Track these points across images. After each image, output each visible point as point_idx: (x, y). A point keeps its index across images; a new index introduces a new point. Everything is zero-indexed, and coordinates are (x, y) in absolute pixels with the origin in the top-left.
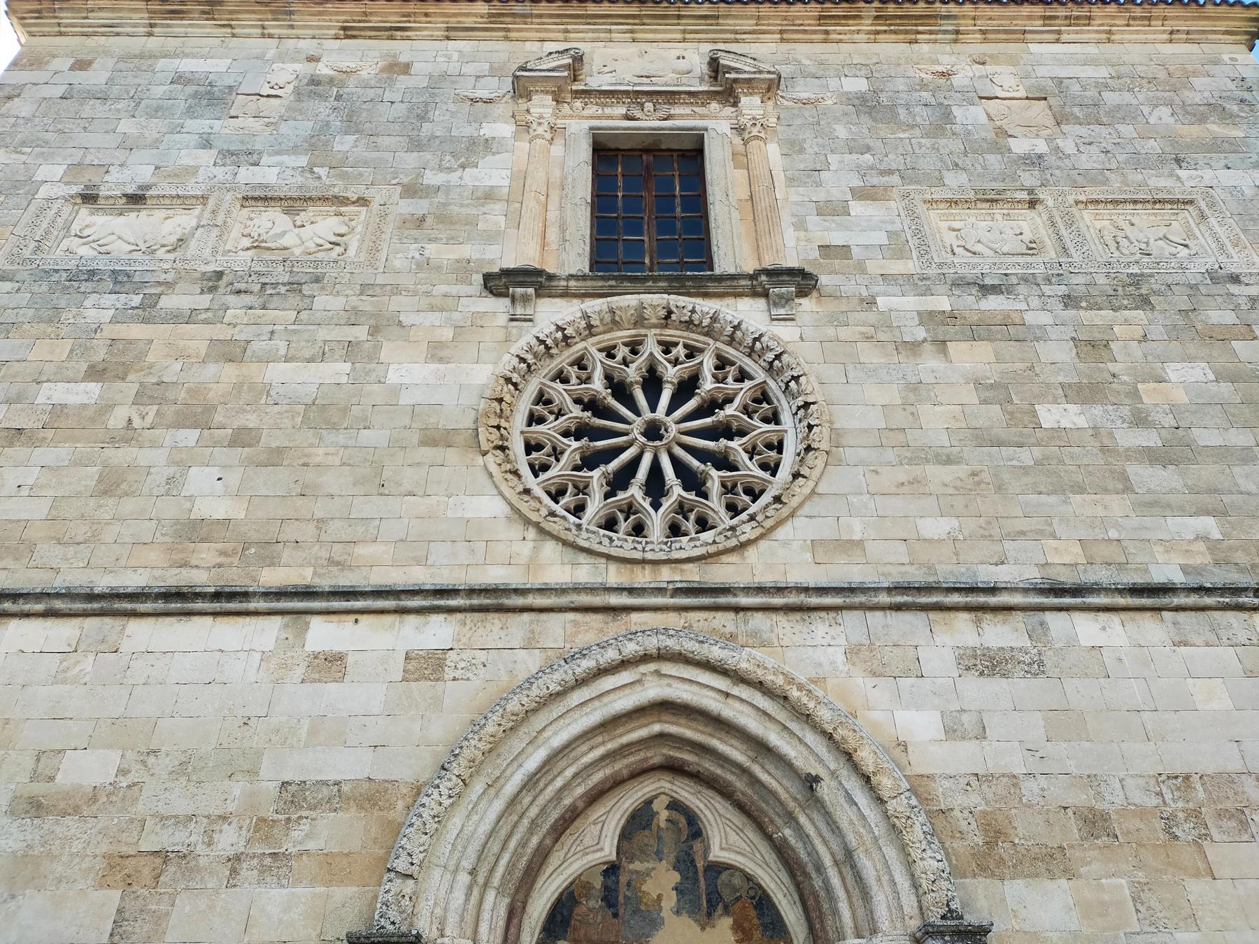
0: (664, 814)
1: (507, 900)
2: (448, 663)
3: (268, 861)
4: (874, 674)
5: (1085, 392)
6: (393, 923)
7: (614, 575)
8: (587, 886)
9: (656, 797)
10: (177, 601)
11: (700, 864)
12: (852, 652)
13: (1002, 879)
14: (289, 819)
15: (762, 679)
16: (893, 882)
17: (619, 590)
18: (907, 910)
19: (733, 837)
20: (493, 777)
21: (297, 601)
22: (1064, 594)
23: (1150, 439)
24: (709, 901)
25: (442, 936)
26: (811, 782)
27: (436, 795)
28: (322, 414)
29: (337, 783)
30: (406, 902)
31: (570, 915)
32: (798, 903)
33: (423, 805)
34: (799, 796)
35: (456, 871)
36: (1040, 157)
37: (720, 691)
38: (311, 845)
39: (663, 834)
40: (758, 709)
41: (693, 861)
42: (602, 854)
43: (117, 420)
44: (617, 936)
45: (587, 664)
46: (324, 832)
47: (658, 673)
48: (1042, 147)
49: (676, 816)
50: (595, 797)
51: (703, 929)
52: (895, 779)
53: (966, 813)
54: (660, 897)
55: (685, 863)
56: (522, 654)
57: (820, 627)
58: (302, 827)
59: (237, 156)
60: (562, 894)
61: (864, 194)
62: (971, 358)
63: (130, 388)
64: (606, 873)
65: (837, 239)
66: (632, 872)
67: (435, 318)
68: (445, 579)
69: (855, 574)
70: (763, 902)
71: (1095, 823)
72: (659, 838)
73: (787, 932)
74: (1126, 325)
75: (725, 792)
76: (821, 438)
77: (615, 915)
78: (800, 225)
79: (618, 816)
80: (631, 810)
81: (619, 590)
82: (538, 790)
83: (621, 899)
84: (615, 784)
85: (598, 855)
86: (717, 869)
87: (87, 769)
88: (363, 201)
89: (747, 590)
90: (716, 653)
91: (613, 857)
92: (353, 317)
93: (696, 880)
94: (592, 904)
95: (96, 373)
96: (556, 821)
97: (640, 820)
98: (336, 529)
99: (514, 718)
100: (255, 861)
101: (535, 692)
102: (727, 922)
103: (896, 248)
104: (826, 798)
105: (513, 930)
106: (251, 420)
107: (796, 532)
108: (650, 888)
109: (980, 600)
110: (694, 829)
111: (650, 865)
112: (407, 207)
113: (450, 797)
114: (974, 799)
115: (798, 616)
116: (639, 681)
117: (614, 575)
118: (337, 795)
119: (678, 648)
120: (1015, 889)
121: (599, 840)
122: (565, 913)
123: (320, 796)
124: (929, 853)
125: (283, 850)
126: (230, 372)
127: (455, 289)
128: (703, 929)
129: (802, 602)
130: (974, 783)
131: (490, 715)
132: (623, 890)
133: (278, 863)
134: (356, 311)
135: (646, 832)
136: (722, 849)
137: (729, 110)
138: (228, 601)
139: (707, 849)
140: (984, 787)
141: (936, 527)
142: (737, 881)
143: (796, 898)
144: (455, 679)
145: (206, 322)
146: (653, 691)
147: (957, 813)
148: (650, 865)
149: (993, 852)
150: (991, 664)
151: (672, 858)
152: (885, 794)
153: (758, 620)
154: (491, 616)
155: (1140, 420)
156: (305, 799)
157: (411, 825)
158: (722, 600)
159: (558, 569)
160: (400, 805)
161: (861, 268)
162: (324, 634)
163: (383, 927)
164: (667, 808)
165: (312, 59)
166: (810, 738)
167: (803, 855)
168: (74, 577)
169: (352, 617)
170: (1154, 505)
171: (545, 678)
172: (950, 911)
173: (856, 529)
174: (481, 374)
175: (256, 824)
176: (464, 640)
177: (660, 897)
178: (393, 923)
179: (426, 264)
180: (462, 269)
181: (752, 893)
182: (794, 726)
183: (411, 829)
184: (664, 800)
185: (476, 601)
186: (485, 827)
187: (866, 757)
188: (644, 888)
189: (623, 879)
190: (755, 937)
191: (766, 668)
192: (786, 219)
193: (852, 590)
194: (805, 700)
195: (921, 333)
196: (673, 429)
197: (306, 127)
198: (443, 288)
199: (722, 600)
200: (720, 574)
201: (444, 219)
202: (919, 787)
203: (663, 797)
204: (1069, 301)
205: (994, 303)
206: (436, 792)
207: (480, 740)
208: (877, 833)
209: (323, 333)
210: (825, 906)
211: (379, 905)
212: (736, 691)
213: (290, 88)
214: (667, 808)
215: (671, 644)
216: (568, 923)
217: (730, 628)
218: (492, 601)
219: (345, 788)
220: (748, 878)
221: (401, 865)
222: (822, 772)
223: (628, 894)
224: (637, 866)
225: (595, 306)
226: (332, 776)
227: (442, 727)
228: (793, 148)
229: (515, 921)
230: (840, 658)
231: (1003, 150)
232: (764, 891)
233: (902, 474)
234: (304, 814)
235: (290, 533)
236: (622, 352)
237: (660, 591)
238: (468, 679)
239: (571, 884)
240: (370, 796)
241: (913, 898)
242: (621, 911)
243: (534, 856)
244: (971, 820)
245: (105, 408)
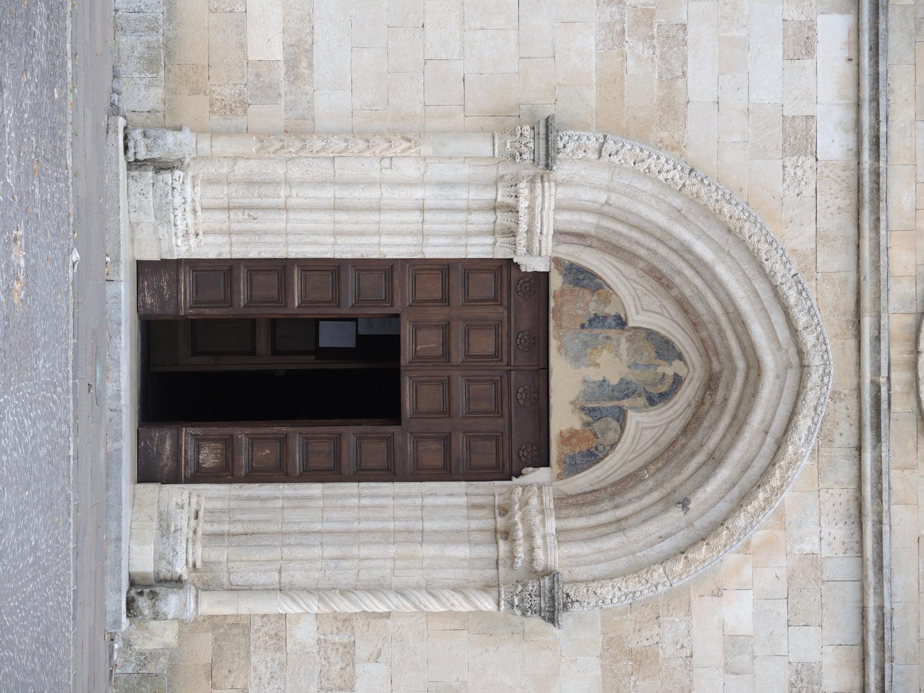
0: (669, 370)
1: (592, 231)
2: (802, 158)
3: (618, 28)
4: (790, 578)
6: (565, 146)
8: (607, 301)
9: (686, 364)
11: (625, 403)
12: (813, 560)
13: (601, 657)
14: (653, 38)
15: (777, 465)
16: (597, 562)
17: (878, 327)
18: (576, 570)
19: (648, 435)
20: (687, 214)
24: (594, 409)
25: (557, 185)
26: (684, 504)
27: (666, 167)
29: (684, 74)
30: (581, 154)
31: (583, 287)
32: (591, 488)
33: (658, 158)
34: (677, 495)
35: (609, 190)
37: (770, 425)
38: (631, 63)
39: (652, 369)
40: (752, 461)
41: (627, 396)
42: (634, 314)
44: (566, 327)
45: (792, 297)
46: (641, 67)
47: (789, 366)
49: (668, 382)
50: (683, 305)
51: (572, 403)
52: (681, 575)
53: (657, 639)
54: (597, 365)
55: (626, 390)
56: (810, 230)
57: (838, 533)
58: (646, 50)
60: (600, 278)
64: (618, 317)
66: (619, 340)
70: (592, 457)
72: (648, 366)
73: (568, 476)
75: (687, 430)
77: (583, 326)
79: (667, 328)
80: (673, 340)
81: (878, 327)
82: (683, 253)
83: (596, 331)
84: (694, 322)
85: (633, 310)
86: (621, 417)
89: (878, 460)
90: (804, 423)
91: (631, 324)
93: (611, 399)
94: (593, 305)
96: (660, 271)
97: (665, 348)
99: (738, 230)
100: (617, 17)
101: (764, 247)
102: (577, 425)
104: (669, 514)
105: (568, 238)
108: (605, 357)
111: (624, 357)
113: (666, 180)
114: (668, 650)
115: (854, 511)
116: (780, 348)
118: (673, 78)
119: (809, 385)
120: (593, 666)
121: (646, 311)
122: (584, 282)
123: (673, 61)
124: (618, 593)
125: (627, 38)
128: (572, 403)
130: (686, 652)
131: (740, 208)
132: (602, 333)
133: (615, 36)
135: (653, 354)
136: (638, 423)
139: (637, 409)
140: (680, 661)
142: (611, 436)
143: (596, 487)
144: (784, 167)
146: (769, 360)
147: (656, 630)
148: (624, 357)
151: (630, 378)
152: (668, 565)
153: (845, 470)
154: (853, 195)
156: (671, 48)
157: (642, 150)
158: (868, 434)
160: (664, 134)
163: (561, 139)
164: (675, 374)
166: (723, 506)
167: (630, 495)
169: (853, 55)
171: (778, 256)
172: (573, 602)
175: (648, 10)
176: (827, 171)
177: (597, 365)
178: (565, 146)
181: (600, 448)
182: (735, 493)
183: (638, 150)
184: (682, 373)
185: (867, 179)
186: (644, 210)
187: (703, 551)
188: (605, 351)
189: (613, 333)
190: (565, 448)
191: (788, 469)
193: (880, 569)
194: (755, 504)
199: (868, 434)
202: (680, 600)
203: (686, 372)
206: (670, 166)
207: (717, 201)
208: (638, 554)
210: (587, 510)
211: (578, 133)
212: (770, 440)
214: (675, 374)
215: (814, 378)
216: (576, 285)
217: (839, 441)
219: (680, 83)
220: (613, 446)
221: (610, 146)
222: (692, 514)
223: (600, 338)
224: (624, 345)
226: (690, 69)
229: (576, 240)
230: (807, 548)
232: (602, 459)
234: (658, 52)
237: (877, 370)
238: (784, 180)
239: (609, 286)
240: (672, 107)
241: (585, 577)
242: (585, 332)
243: (630, 253)
244: (650, 642)
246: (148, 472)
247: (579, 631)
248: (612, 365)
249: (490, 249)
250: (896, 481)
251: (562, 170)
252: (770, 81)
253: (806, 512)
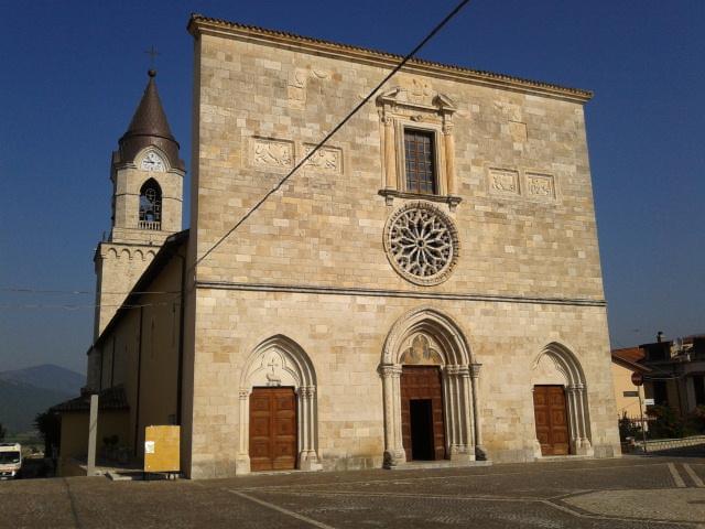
5: (516, 243)
7: (417, 289)
10: (330, 291)
21: (354, 292)
22: (502, 298)
23: (525, 257)
28: (346, 234)
36: (520, 152)
43: (297, 232)
48: (521, 149)
55: (424, 348)
59: (298, 122)
61: (476, 163)
62: (492, 230)
63: (296, 222)
65: (467, 181)
67: (367, 202)
68: (383, 287)
69: (464, 290)
71: (499, 345)
74: (529, 220)
76: (460, 252)
78: (458, 175)
86: (430, 349)
87: (322, 329)
88: (339, 148)
92: (347, 200)
95: (286, 216)
97: (416, 339)
98: (356, 272)
103: (480, 188)
106: (329, 236)
107: (453, 278)
109: (487, 298)
110: (426, 342)
112: (352, 153)
117: (417, 289)
120: (485, 357)
126: (321, 219)
127: (372, 191)
129: (453, 297)
134: (347, 198)
137: (440, 118)
138: (340, 291)
141: (481, 279)
145: (310, 198)
149: (482, 351)
150: (486, 313)
155: (525, 252)
159: (406, 287)
161: (472, 194)
162: (360, 300)
165: (308, 67)
168: (302, 282)
170: (522, 277)
173: (465, 278)
174: (382, 224)
179: (362, 180)
180: (373, 183)
192: (454, 171)
195: (483, 219)
196: (426, 242)
197: (313, 108)
198: (368, 191)
200: (439, 289)
201: (365, 161)
204: (518, 211)
205: (501, 210)
209: (341, 206)
213: (304, 85)
218: (394, 294)
225: (409, 202)
227: (387, 324)
228: (457, 139)
231: (511, 146)
233: (474, 264)
235: (346, 273)
236: (411, 215)
240: (376, 338)
245: (292, 229)
246: (446, 457)
247: (484, 360)
248: (420, 351)
249: (396, 376)
250: (447, 291)
251: (390, 362)
252: (370, 315)
253: (454, 309)
